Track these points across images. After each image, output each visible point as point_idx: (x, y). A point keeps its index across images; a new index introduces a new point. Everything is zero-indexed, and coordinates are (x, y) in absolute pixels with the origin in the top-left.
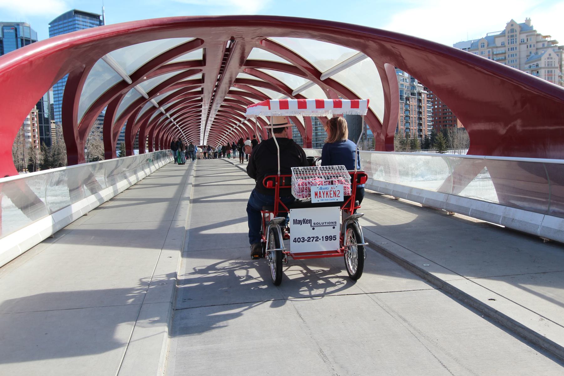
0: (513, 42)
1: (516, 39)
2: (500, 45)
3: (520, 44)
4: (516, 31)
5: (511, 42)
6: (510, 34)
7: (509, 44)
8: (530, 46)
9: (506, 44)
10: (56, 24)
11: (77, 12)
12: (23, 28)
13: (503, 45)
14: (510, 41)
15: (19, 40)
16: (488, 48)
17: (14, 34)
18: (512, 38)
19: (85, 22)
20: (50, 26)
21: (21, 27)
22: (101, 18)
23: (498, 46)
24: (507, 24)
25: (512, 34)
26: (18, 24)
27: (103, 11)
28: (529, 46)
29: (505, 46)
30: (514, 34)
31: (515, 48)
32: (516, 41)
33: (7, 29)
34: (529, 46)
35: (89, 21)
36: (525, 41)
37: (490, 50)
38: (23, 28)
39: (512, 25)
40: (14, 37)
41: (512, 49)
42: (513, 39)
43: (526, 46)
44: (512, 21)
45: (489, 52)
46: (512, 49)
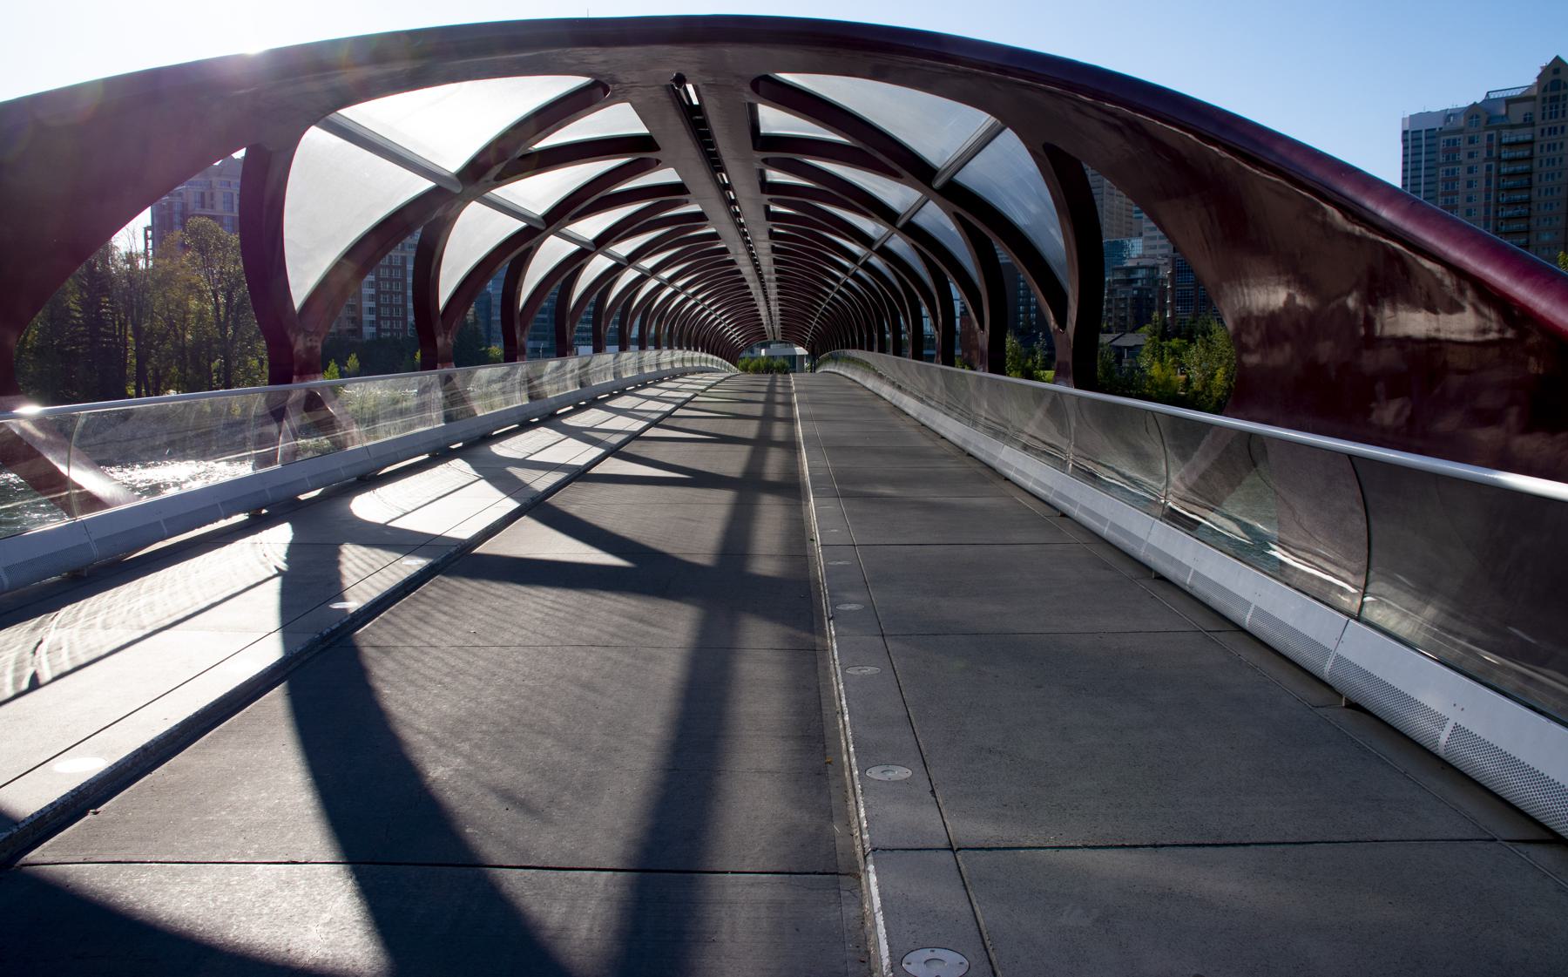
0: (1556, 113)
1: (1564, 106)
2: (1520, 121)
5: (1551, 113)
7: (1543, 118)
9: (1537, 119)
13: (1528, 122)
14: (1547, 112)
16: (1487, 129)
18: (1554, 104)
24: (1542, 67)
25: (1555, 93)
29: (1533, 125)
31: (1559, 130)
32: (1564, 112)
37: (1494, 132)
39: (1556, 71)
41: (1552, 131)
42: (1557, 107)
44: (1557, 59)
45: (1490, 137)
46: (1552, 131)
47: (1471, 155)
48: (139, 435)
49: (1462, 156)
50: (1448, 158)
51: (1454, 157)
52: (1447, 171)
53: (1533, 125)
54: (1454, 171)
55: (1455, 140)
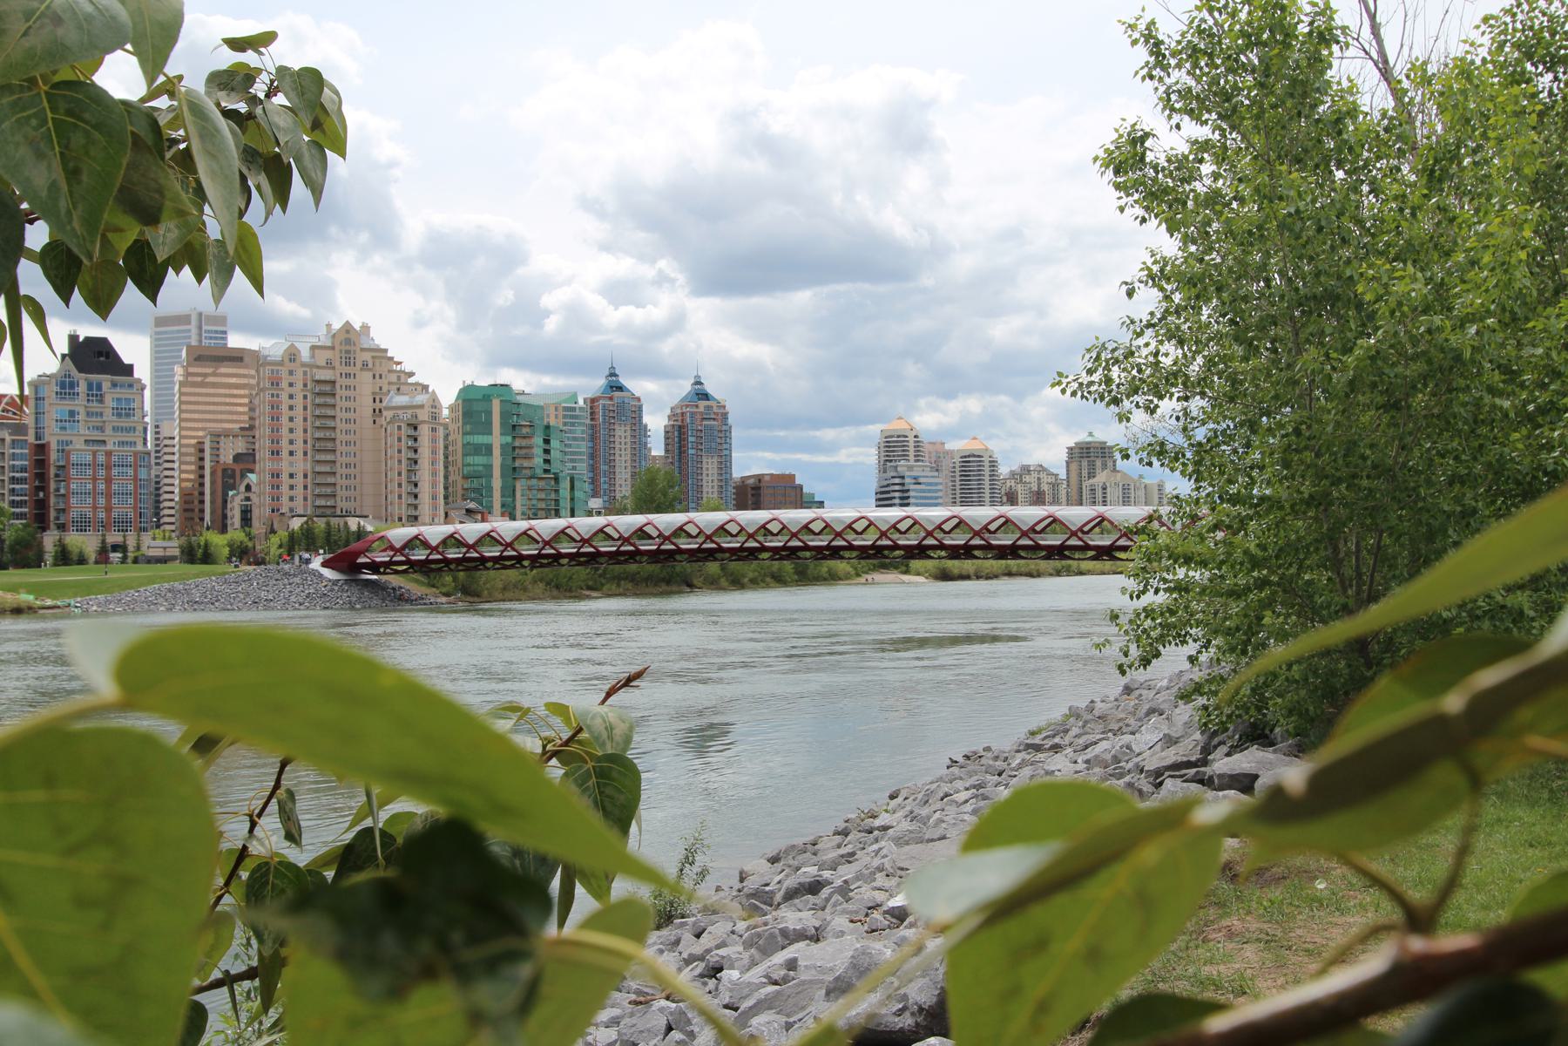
3: (361, 369)
4: (355, 345)
6: (344, 348)
8: (381, 377)
9: (337, 364)
13: (329, 365)
14: (344, 360)
18: (348, 356)
23: (319, 364)
25: (348, 348)
28: (377, 376)
29: (334, 368)
30: (352, 348)
34: (377, 376)
36: (370, 366)
41: (348, 375)
43: (371, 374)
46: (348, 375)
47: (291, 385)
48: (1043, 772)
49: (284, 384)
50: (272, 384)
51: (278, 384)
52: (273, 395)
53: (334, 368)
54: (278, 396)
55: (278, 371)
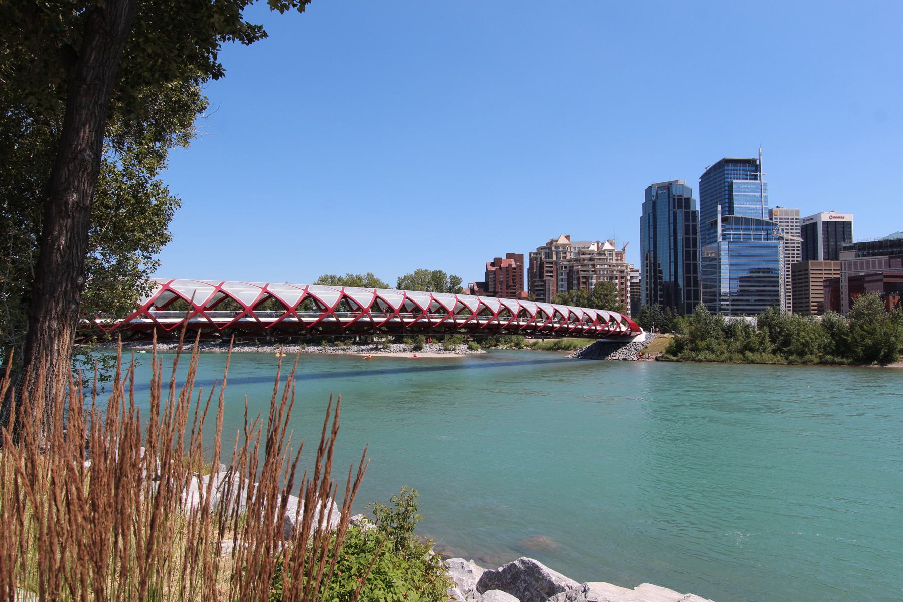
10: (707, 177)
11: (727, 161)
12: (676, 187)
15: (671, 199)
17: (667, 194)
19: (737, 170)
20: (700, 180)
21: (674, 186)
22: (757, 163)
26: (671, 184)
27: (759, 155)
33: (660, 190)
35: (741, 168)
38: (676, 187)
40: (667, 197)
